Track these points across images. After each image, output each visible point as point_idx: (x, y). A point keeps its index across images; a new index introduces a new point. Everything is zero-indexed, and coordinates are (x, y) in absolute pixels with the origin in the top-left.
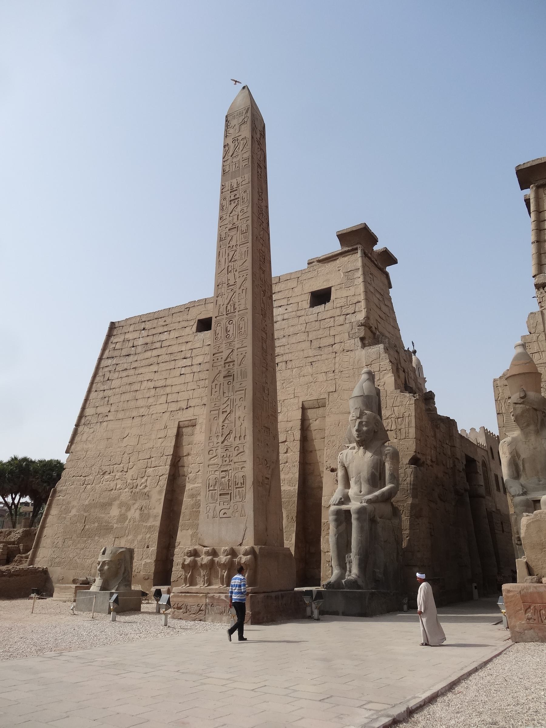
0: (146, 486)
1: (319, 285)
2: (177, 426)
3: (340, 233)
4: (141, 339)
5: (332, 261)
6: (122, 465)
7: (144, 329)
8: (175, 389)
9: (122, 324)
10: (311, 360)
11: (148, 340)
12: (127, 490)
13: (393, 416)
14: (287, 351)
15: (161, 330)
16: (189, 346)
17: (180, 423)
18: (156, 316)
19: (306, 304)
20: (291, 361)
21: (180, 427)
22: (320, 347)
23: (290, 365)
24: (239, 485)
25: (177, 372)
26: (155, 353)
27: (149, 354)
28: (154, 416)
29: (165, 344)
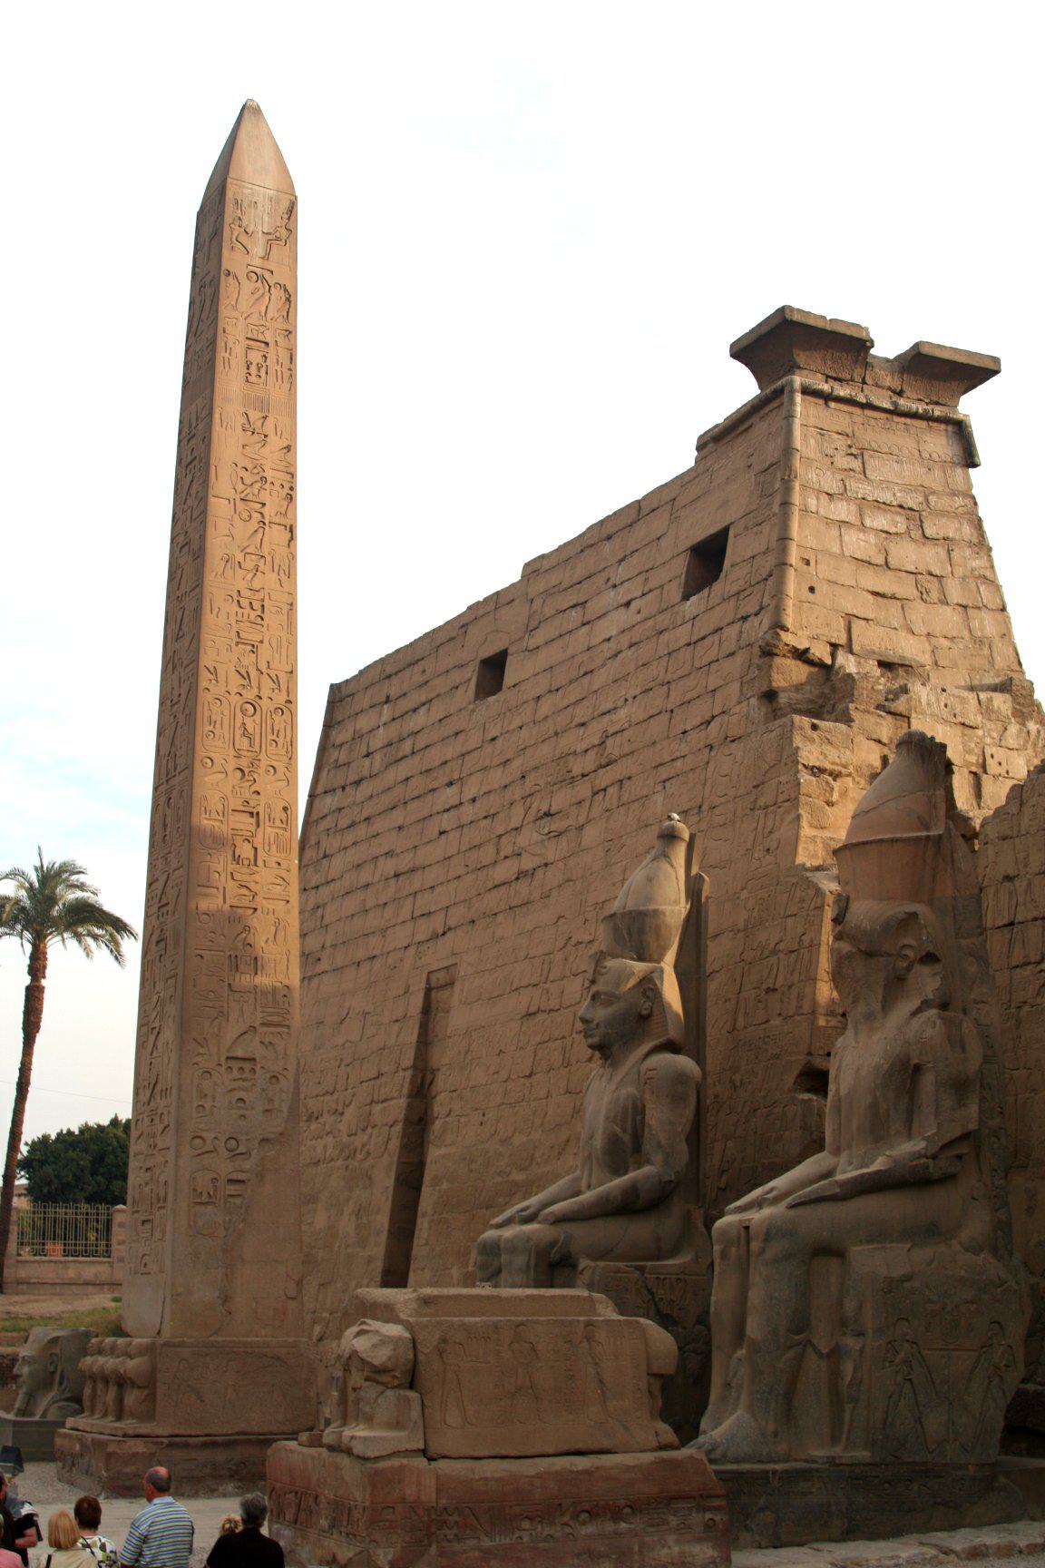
0: (368, 1153)
1: (701, 529)
2: (423, 985)
3: (734, 350)
4: (381, 730)
5: (741, 433)
6: (335, 1096)
7: (388, 700)
8: (432, 875)
9: (351, 689)
10: (664, 773)
11: (393, 732)
12: (340, 1162)
13: (781, 947)
14: (627, 749)
15: (416, 698)
16: (457, 747)
17: (431, 976)
18: (409, 659)
19: (675, 591)
20: (630, 778)
21: (433, 989)
22: (685, 732)
23: (632, 789)
24: (205, 1198)
25: (433, 828)
26: (403, 770)
27: (392, 776)
28: (390, 960)
29: (421, 741)
